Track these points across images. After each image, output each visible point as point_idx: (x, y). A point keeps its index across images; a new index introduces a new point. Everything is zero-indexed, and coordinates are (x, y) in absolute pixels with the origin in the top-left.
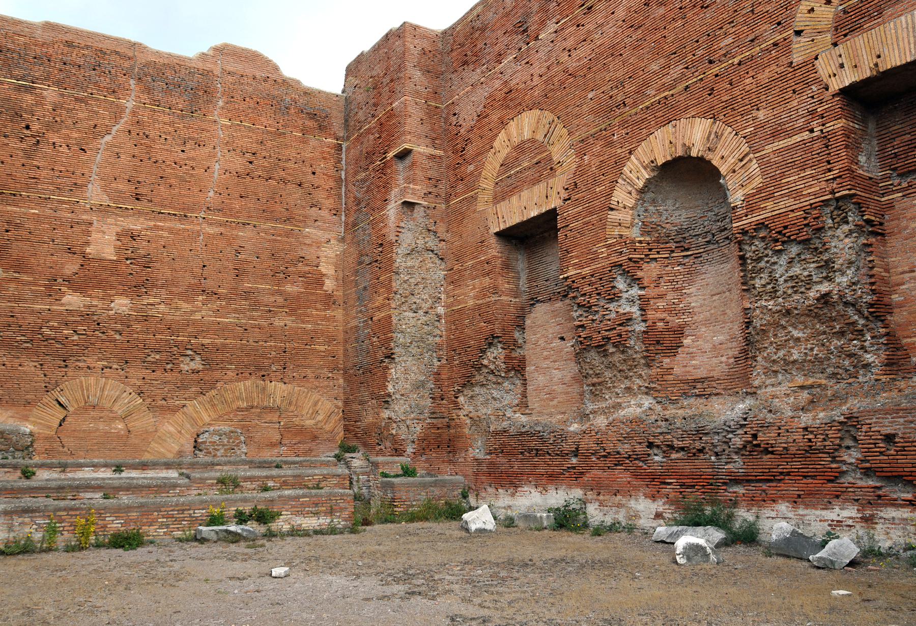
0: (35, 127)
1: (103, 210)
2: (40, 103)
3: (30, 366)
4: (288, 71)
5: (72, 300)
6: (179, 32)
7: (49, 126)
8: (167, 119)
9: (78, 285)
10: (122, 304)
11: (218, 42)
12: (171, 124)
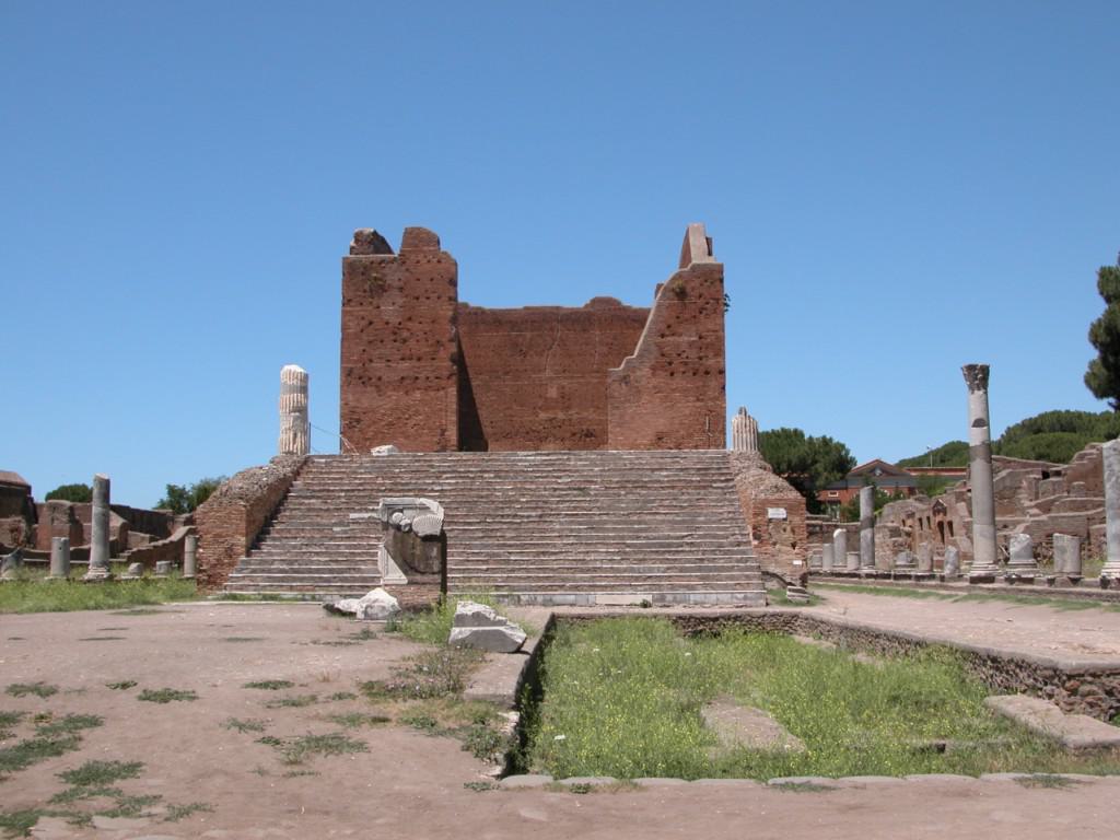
4: (626, 303)
5: (543, 415)
9: (546, 409)
10: (561, 416)
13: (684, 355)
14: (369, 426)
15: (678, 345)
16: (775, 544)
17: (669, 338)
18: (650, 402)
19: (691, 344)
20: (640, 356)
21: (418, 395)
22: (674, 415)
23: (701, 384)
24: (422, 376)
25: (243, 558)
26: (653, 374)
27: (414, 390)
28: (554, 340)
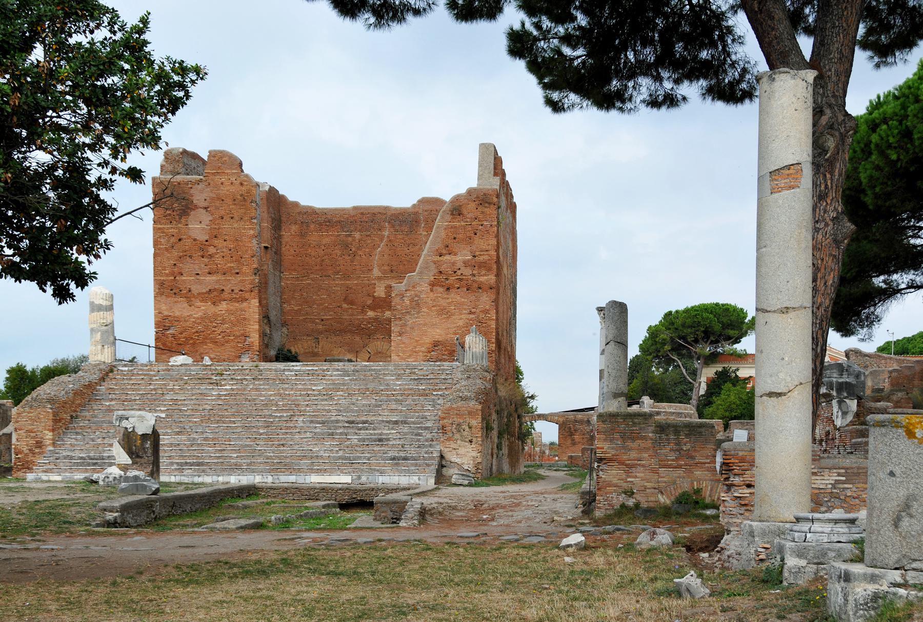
0: (353, 249)
1: (379, 278)
2: (354, 240)
3: (358, 339)
5: (371, 314)
6: (402, 198)
7: (358, 249)
8: (401, 237)
9: (373, 308)
11: (420, 197)
12: (403, 239)
13: (459, 272)
14: (181, 334)
15: (454, 264)
16: (457, 440)
17: (447, 257)
18: (428, 314)
19: (464, 262)
20: (421, 273)
21: (224, 306)
22: (449, 326)
23: (473, 298)
24: (227, 289)
25: (51, 448)
26: (432, 290)
27: (220, 301)
28: (382, 240)
